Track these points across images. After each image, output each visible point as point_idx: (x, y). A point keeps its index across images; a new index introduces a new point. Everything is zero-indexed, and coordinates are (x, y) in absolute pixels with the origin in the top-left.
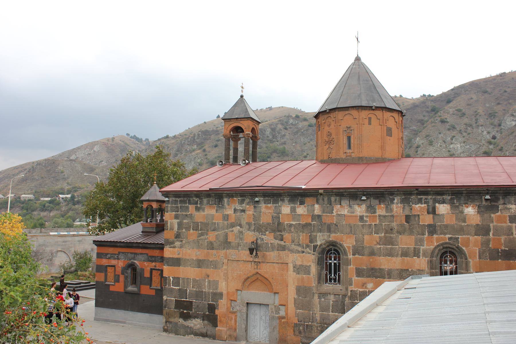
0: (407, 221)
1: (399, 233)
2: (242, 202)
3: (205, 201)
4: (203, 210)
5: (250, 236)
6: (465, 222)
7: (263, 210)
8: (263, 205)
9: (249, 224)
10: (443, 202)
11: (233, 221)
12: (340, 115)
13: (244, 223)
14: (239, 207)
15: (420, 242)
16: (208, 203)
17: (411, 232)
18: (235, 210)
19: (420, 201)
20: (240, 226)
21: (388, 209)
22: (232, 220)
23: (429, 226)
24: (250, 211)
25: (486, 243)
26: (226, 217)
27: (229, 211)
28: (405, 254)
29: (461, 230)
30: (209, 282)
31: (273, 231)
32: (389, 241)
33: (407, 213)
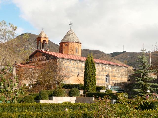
0: (102, 69)
1: (101, 71)
2: (75, 62)
3: (67, 60)
4: (67, 63)
5: (77, 70)
6: (109, 70)
7: (79, 64)
8: (79, 63)
9: (76, 67)
10: (107, 66)
11: (73, 66)
12: (75, 43)
13: (75, 67)
14: (74, 63)
15: (104, 73)
16: (68, 61)
17: (103, 72)
18: (73, 64)
19: (104, 66)
20: (75, 67)
21: (100, 67)
22: (73, 66)
23: (105, 71)
24: (77, 64)
25: (112, 74)
26: (72, 65)
27: (72, 64)
28: (102, 76)
29: (109, 72)
30: (68, 81)
31: (81, 69)
32: (100, 73)
33: (102, 68)
